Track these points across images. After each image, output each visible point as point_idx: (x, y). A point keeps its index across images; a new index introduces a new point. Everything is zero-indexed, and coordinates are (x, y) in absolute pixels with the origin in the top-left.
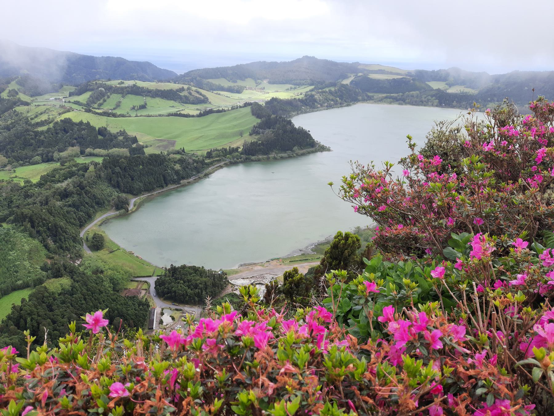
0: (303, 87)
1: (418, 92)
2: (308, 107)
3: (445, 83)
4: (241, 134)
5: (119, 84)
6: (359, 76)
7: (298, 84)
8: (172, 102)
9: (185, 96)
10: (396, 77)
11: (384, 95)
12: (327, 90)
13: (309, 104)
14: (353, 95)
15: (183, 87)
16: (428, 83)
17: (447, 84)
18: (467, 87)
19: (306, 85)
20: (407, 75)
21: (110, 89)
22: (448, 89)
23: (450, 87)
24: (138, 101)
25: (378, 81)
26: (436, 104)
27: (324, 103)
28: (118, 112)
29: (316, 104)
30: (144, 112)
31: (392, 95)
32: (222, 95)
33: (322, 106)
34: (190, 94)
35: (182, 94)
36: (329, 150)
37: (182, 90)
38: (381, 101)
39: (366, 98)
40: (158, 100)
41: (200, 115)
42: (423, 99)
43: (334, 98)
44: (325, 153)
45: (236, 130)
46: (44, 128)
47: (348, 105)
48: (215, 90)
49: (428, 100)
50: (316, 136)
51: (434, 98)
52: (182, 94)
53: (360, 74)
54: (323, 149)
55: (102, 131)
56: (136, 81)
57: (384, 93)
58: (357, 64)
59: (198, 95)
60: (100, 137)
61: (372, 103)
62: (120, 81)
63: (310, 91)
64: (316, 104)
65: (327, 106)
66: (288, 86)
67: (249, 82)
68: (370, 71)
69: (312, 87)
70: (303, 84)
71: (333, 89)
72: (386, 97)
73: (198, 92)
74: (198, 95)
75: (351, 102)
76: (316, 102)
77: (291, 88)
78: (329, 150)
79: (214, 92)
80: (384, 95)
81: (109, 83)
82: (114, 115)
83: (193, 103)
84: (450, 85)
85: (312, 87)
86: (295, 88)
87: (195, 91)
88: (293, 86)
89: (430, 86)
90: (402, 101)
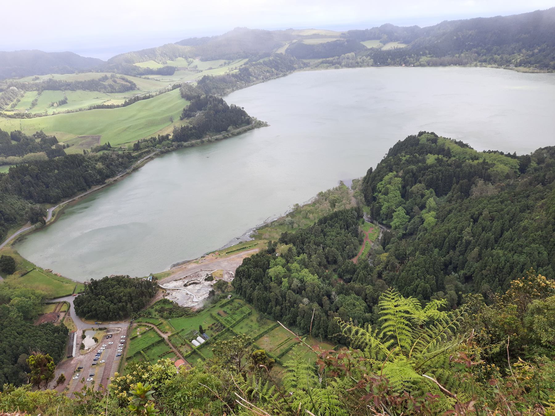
0: (237, 61)
1: (353, 54)
2: (243, 82)
3: (379, 41)
4: (171, 120)
5: (33, 80)
7: (230, 58)
8: (96, 92)
9: (110, 85)
10: (330, 40)
11: (320, 60)
12: (261, 61)
13: (244, 78)
14: (289, 64)
15: (106, 76)
16: (362, 43)
17: (381, 42)
18: (400, 43)
19: (240, 58)
20: (341, 37)
22: (382, 47)
23: (384, 44)
24: (59, 96)
25: (311, 47)
26: (371, 64)
27: (259, 75)
29: (251, 77)
31: (328, 59)
32: (152, 79)
33: (257, 78)
35: (106, 83)
36: (266, 125)
38: (317, 66)
39: (302, 65)
41: (126, 104)
42: (359, 60)
43: (268, 68)
44: (262, 129)
45: (167, 115)
47: (285, 75)
48: (143, 74)
49: (363, 60)
50: (251, 112)
51: (369, 57)
52: (106, 83)
53: (295, 41)
54: (260, 125)
55: (16, 136)
56: (53, 75)
57: (322, 58)
59: (124, 83)
60: (14, 143)
61: (309, 70)
62: (34, 77)
63: (244, 65)
64: (251, 77)
65: (263, 79)
66: (222, 62)
68: (304, 36)
69: (247, 60)
70: (237, 58)
71: (266, 59)
72: (322, 63)
74: (124, 83)
75: (287, 71)
76: (251, 75)
77: (225, 63)
78: (266, 125)
79: (143, 77)
80: (320, 60)
82: (28, 116)
83: (120, 92)
84: (385, 43)
85: (247, 60)
86: (229, 63)
87: (120, 78)
88: (227, 61)
89: (364, 46)
90: (336, 64)
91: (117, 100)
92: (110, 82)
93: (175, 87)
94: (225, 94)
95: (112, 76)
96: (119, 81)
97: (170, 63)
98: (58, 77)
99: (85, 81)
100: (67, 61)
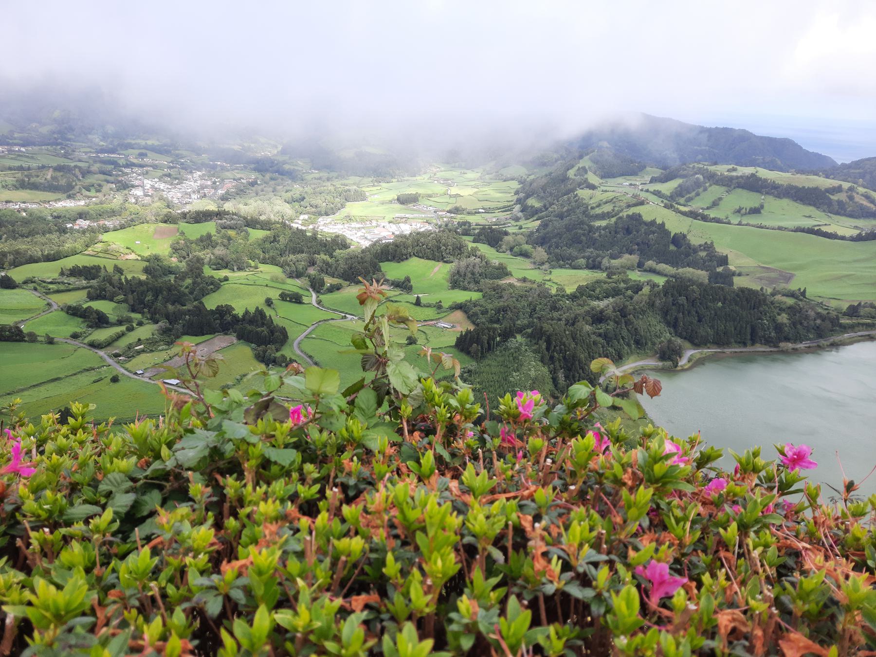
5: (728, 171)
8: (812, 208)
9: (840, 202)
15: (840, 187)
21: (712, 178)
24: (748, 200)
28: (712, 214)
30: (754, 220)
34: (851, 198)
35: (834, 198)
37: (839, 189)
40: (785, 202)
46: (603, 223)
52: (834, 198)
55: (679, 240)
56: (758, 169)
59: (865, 203)
60: (672, 248)
62: (731, 167)
73: (867, 197)
74: (865, 203)
81: (712, 168)
82: (705, 218)
83: (851, 216)
87: (862, 195)
92: (842, 197)
95: (851, 189)
98: (764, 173)
99: (804, 187)
100: (780, 151)
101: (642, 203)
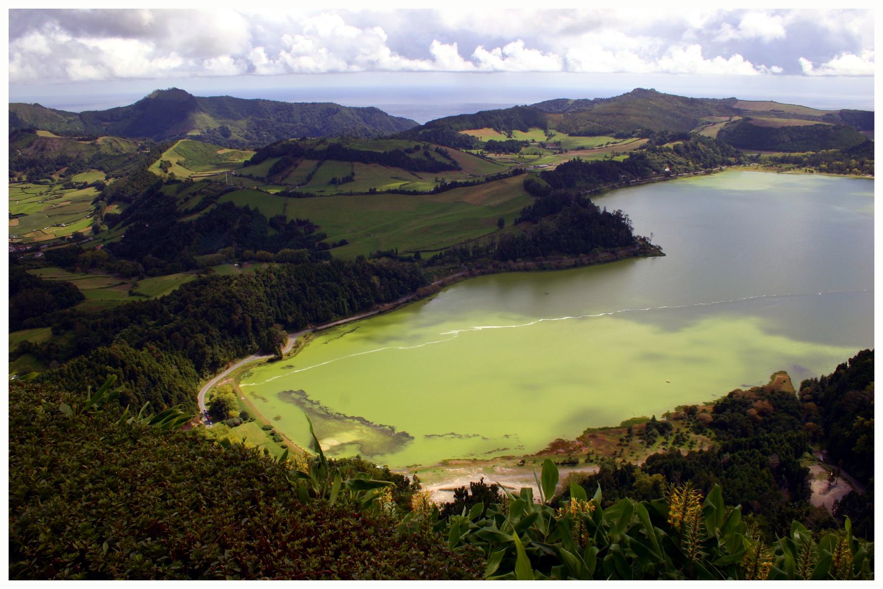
6: (734, 122)
11: (779, 155)
12: (670, 145)
13: (635, 172)
28: (304, 190)
31: (793, 154)
34: (427, 154)
35: (413, 156)
37: (417, 148)
41: (437, 191)
46: (194, 217)
53: (736, 118)
57: (784, 151)
58: (733, 100)
60: (271, 232)
63: (640, 148)
67: (536, 135)
72: (783, 161)
74: (440, 159)
82: (298, 195)
85: (645, 141)
88: (612, 140)
91: (426, 184)
93: (517, 172)
94: (599, 193)
95: (426, 147)
96: (433, 154)
97: (519, 136)
101: (232, 190)
